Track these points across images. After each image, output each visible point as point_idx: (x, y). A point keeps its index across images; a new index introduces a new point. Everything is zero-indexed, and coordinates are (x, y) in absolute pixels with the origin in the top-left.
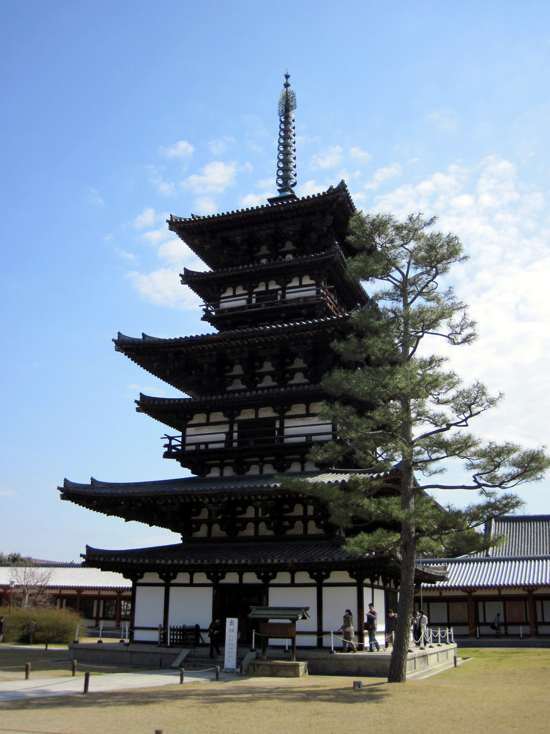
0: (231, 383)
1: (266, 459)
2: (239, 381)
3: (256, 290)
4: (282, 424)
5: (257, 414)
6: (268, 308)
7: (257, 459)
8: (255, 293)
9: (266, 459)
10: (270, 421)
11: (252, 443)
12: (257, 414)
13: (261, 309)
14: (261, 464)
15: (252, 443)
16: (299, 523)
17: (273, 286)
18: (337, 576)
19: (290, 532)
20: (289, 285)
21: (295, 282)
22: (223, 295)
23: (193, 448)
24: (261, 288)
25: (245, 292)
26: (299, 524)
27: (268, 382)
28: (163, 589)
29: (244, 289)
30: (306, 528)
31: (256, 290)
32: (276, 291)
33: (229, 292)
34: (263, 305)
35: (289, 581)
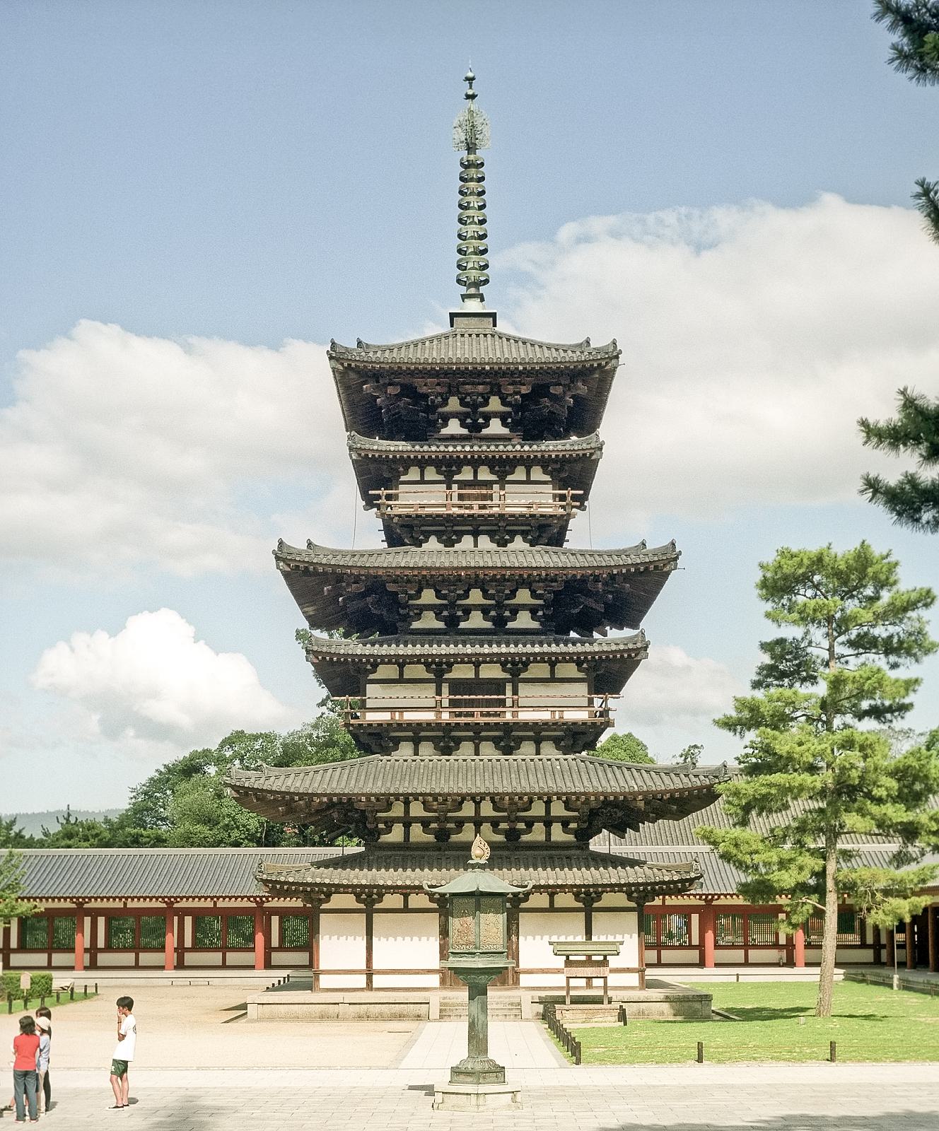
0: (418, 617)
1: (483, 734)
2: (432, 614)
3: (456, 478)
4: (515, 692)
5: (477, 673)
6: (483, 512)
7: (471, 734)
8: (456, 482)
9: (483, 734)
10: (498, 686)
11: (477, 714)
12: (477, 673)
13: (472, 512)
14: (477, 741)
15: (477, 714)
16: (539, 827)
17: (485, 474)
18: (608, 899)
19: (525, 838)
20: (509, 478)
21: (520, 474)
22: (403, 478)
23: (385, 717)
24: (466, 474)
25: (441, 478)
26: (539, 827)
27: (476, 621)
28: (362, 918)
29: (439, 472)
30: (548, 834)
31: (456, 478)
32: (488, 484)
33: (414, 474)
34: (476, 507)
35: (547, 905)
